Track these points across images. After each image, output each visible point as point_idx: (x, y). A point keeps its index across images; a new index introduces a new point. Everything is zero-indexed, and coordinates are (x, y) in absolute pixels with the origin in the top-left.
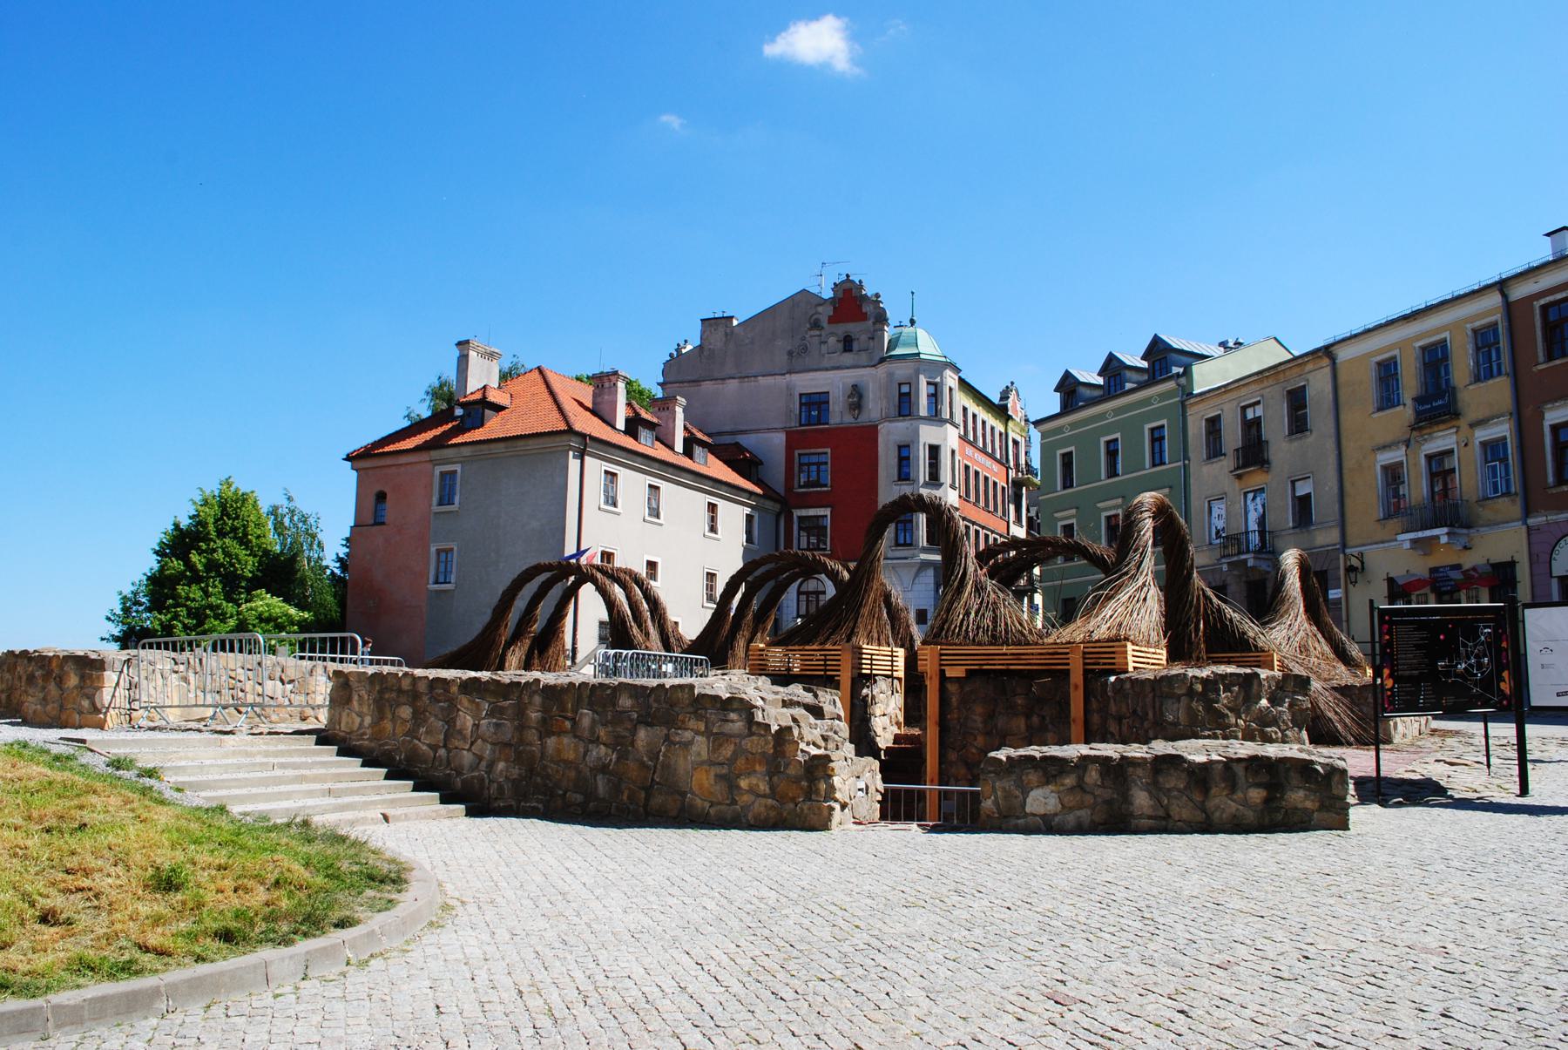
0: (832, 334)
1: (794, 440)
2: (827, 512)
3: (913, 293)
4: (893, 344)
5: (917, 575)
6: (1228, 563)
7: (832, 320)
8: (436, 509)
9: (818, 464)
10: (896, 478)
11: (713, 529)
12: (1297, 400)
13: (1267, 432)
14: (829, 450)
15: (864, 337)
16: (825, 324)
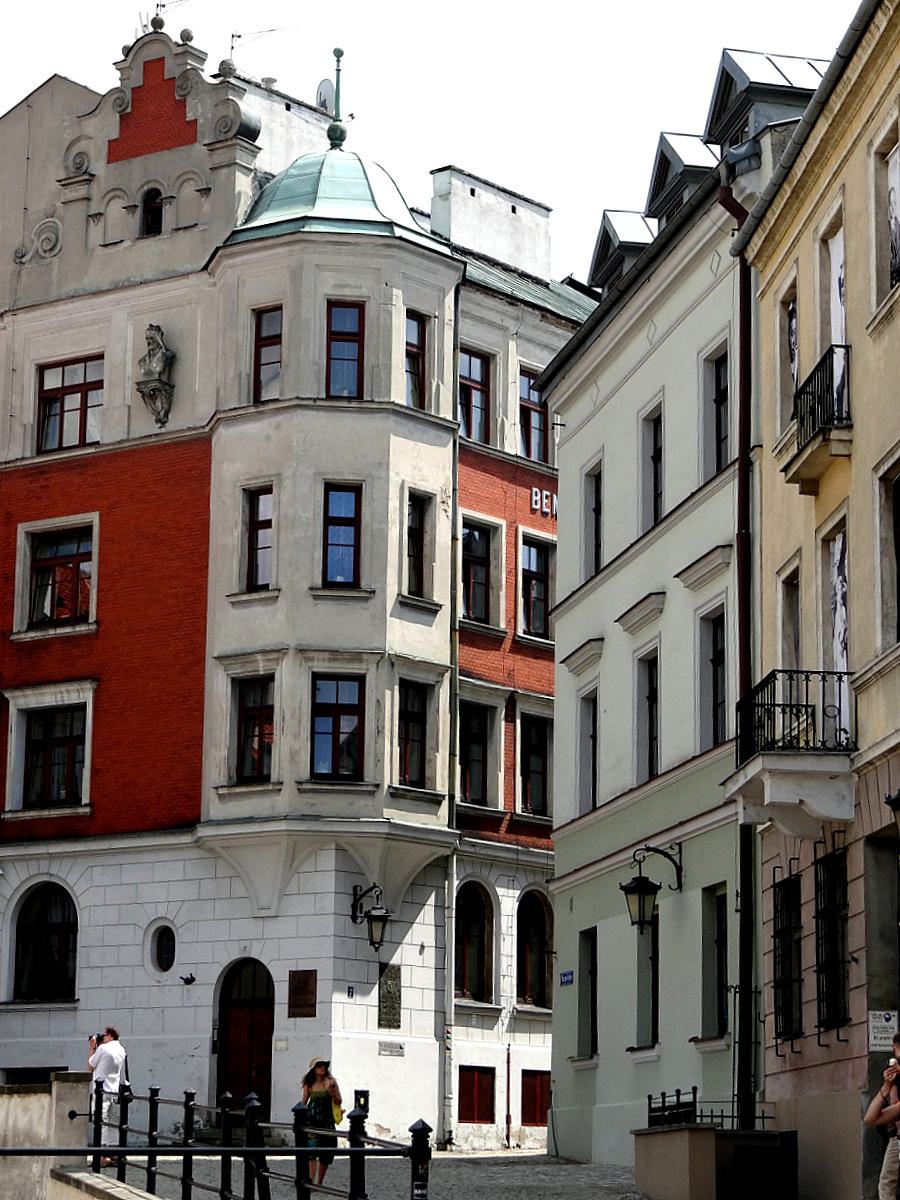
0: (115, 192)
2: (81, 694)
3: (339, 53)
7: (117, 151)
14: (94, 518)
15: (189, 190)
16: (99, 166)
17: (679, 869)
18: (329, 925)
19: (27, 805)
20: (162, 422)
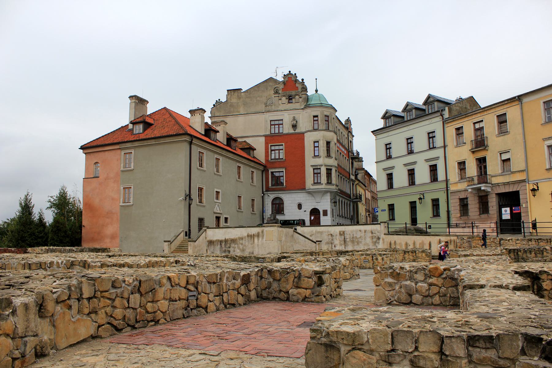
0: (284, 96)
1: (271, 139)
3: (316, 79)
5: (323, 196)
6: (472, 188)
8: (122, 169)
9: (279, 150)
10: (313, 156)
12: (502, 120)
13: (486, 132)
16: (280, 92)
17: (424, 197)
18: (329, 203)
19: (272, 186)
20: (295, 131)
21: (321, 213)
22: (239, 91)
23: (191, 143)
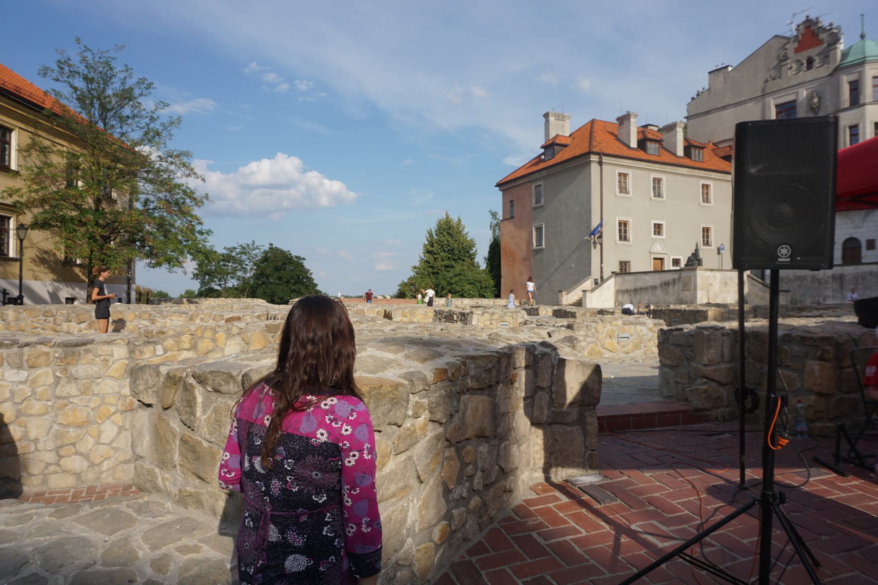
4: (845, 55)
7: (797, 51)
8: (534, 205)
11: (706, 200)
16: (791, 54)
21: (864, 245)
22: (725, 70)
23: (600, 163)
